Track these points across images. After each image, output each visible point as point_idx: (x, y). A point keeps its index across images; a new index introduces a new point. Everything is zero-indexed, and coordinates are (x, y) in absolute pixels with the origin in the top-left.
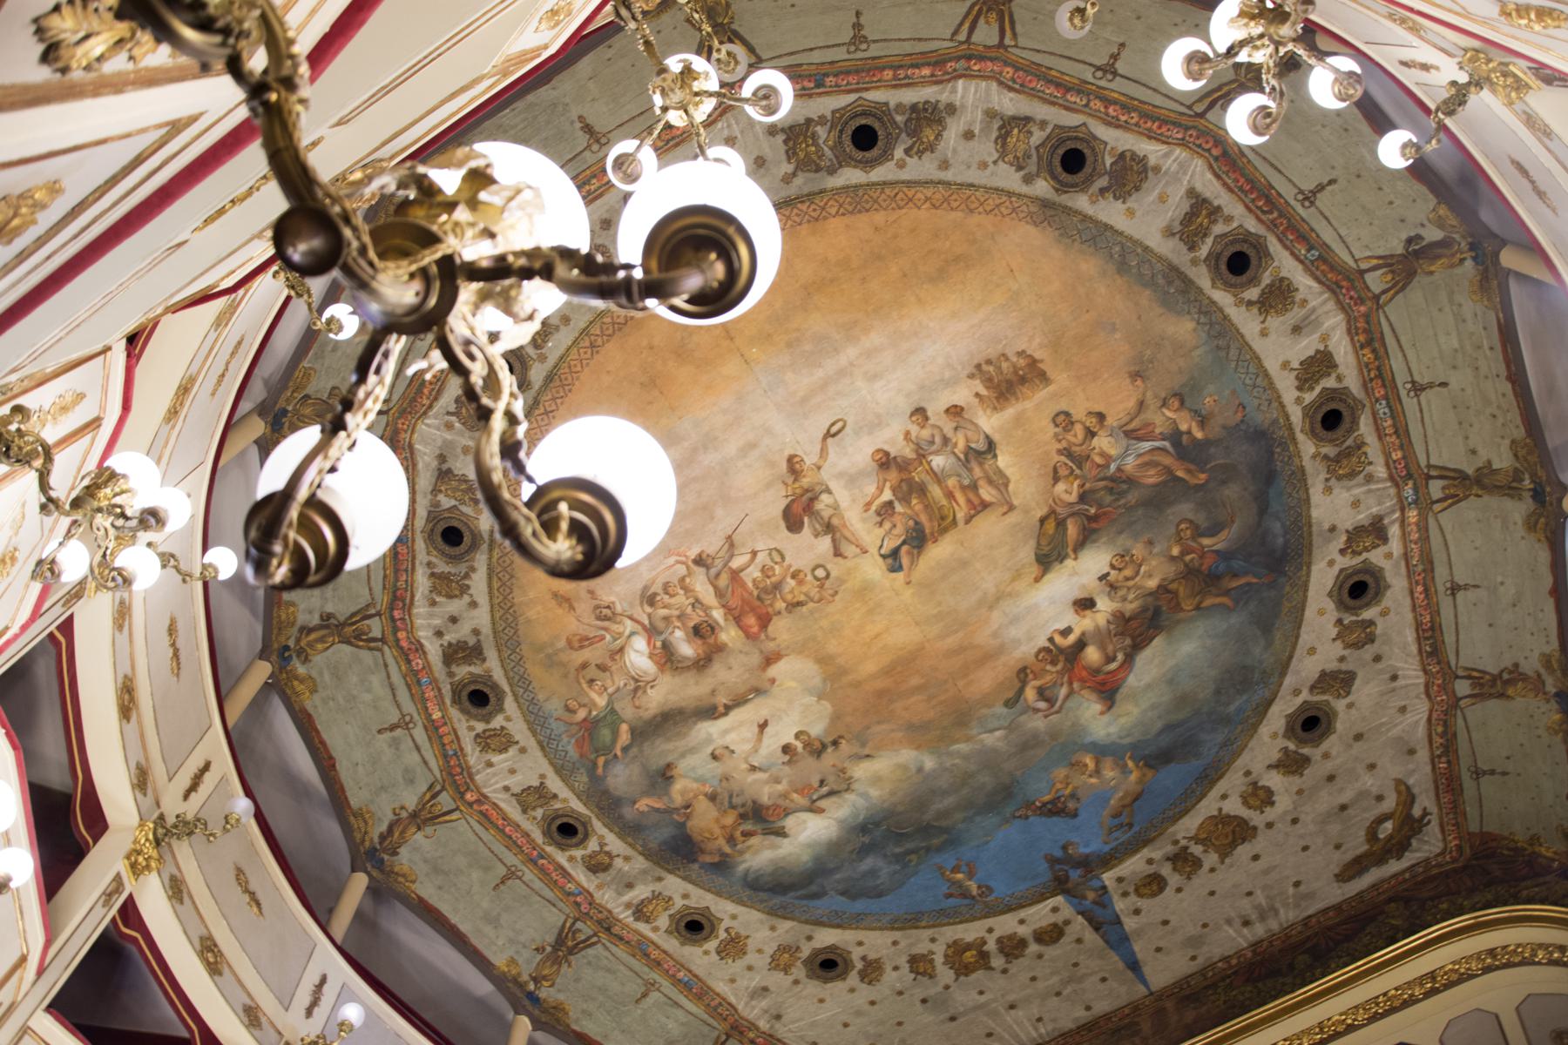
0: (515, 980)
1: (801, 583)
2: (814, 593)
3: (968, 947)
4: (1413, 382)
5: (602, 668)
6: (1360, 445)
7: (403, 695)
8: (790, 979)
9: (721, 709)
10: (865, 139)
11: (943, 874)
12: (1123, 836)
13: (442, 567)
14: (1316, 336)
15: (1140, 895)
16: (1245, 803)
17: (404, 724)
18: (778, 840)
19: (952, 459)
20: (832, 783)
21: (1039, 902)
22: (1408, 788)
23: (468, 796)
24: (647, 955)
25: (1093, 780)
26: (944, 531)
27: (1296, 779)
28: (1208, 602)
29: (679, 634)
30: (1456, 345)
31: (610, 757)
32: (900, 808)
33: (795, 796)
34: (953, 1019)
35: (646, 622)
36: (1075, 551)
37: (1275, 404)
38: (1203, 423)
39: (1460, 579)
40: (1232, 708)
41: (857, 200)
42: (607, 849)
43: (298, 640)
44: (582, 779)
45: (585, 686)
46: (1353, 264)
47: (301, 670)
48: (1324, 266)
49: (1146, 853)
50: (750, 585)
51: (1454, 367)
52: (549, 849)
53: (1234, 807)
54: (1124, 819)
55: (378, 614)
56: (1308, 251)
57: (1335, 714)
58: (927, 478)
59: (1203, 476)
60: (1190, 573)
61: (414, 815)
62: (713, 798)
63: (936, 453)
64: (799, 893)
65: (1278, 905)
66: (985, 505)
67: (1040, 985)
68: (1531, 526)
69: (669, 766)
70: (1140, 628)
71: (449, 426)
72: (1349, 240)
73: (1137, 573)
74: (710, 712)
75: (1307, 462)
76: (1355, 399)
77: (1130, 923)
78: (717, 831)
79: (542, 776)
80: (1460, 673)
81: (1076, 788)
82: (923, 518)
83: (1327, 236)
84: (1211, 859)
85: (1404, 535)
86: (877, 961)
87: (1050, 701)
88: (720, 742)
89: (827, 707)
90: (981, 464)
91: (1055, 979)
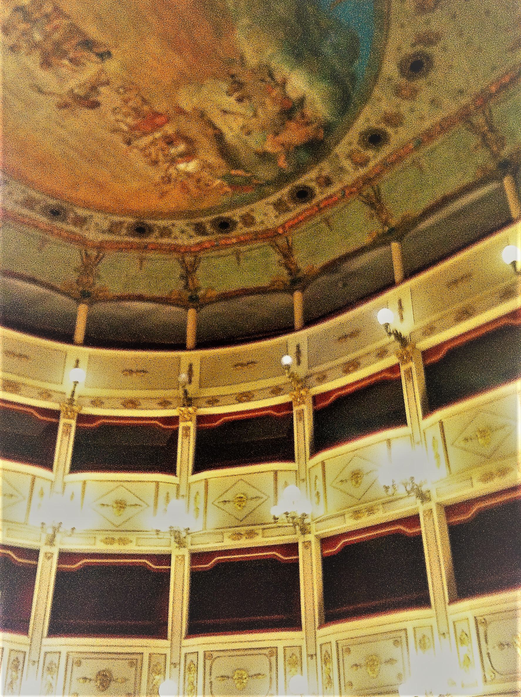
0: (379, 236)
7: (222, 252)
13: (157, 233)
17: (238, 254)
18: (307, 102)
23: (281, 231)
29: (173, 151)
32: (282, 35)
33: (274, 94)
43: (190, 290)
47: (202, 292)
52: (314, 202)
55: (183, 257)
61: (285, 256)
66: (56, 9)
69: (257, 153)
74: (219, 137)
82: (74, 42)
89: (209, 82)
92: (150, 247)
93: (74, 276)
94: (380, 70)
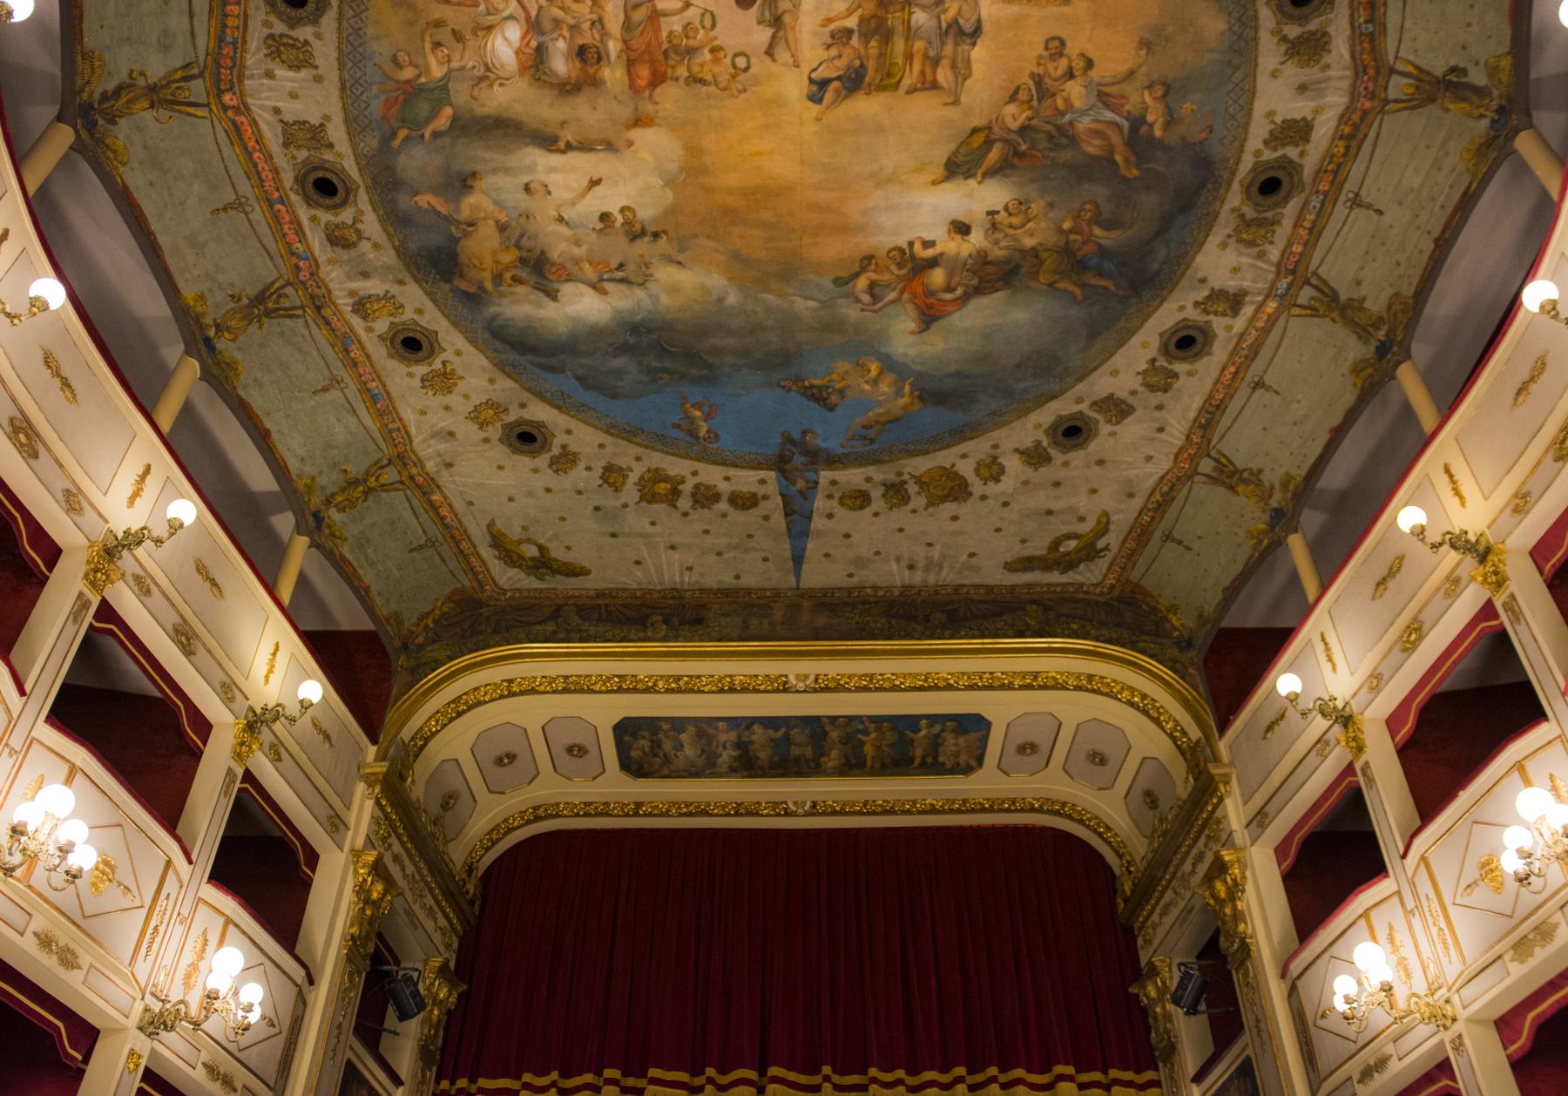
1: (716, 61)
3: (666, 479)
4: (1357, 195)
5: (458, 37)
6: (1275, 222)
8: (483, 435)
9: (562, 145)
11: (683, 405)
12: (860, 447)
14: (1313, 104)
15: (841, 503)
16: (977, 471)
19: (934, 23)
20: (630, 272)
21: (753, 468)
22: (1108, 522)
24: (347, 351)
25: (867, 387)
26: (882, 88)
27: (1029, 471)
28: (1061, 285)
29: (561, 44)
30: (1416, 186)
31: (415, 134)
34: (613, 535)
35: (533, 14)
36: (984, 175)
37: (1237, 144)
38: (1168, 124)
39: (1268, 380)
40: (1021, 385)
42: (359, 226)
44: (372, 142)
45: (428, 45)
46: (1391, 58)
49: (870, 471)
50: (664, 34)
51: (1400, 203)
53: (966, 469)
54: (871, 433)
56: (1366, 22)
57: (1097, 434)
58: (899, 28)
59: (1135, 172)
60: (1066, 251)
62: (502, 228)
63: (924, 8)
65: (945, 564)
66: (935, 86)
67: (709, 539)
68: (1356, 370)
69: (474, 174)
72: (1406, 35)
73: (1023, 226)
74: (548, 141)
75: (1225, 212)
76: (1301, 180)
77: (818, 522)
78: (489, 263)
79: (327, 118)
80: (1213, 454)
81: (847, 386)
82: (871, 66)
83: (1393, 18)
84: (919, 501)
86: (575, 454)
87: (875, 298)
88: (540, 176)
90: (956, 44)
91: (725, 541)
94: (551, 404)
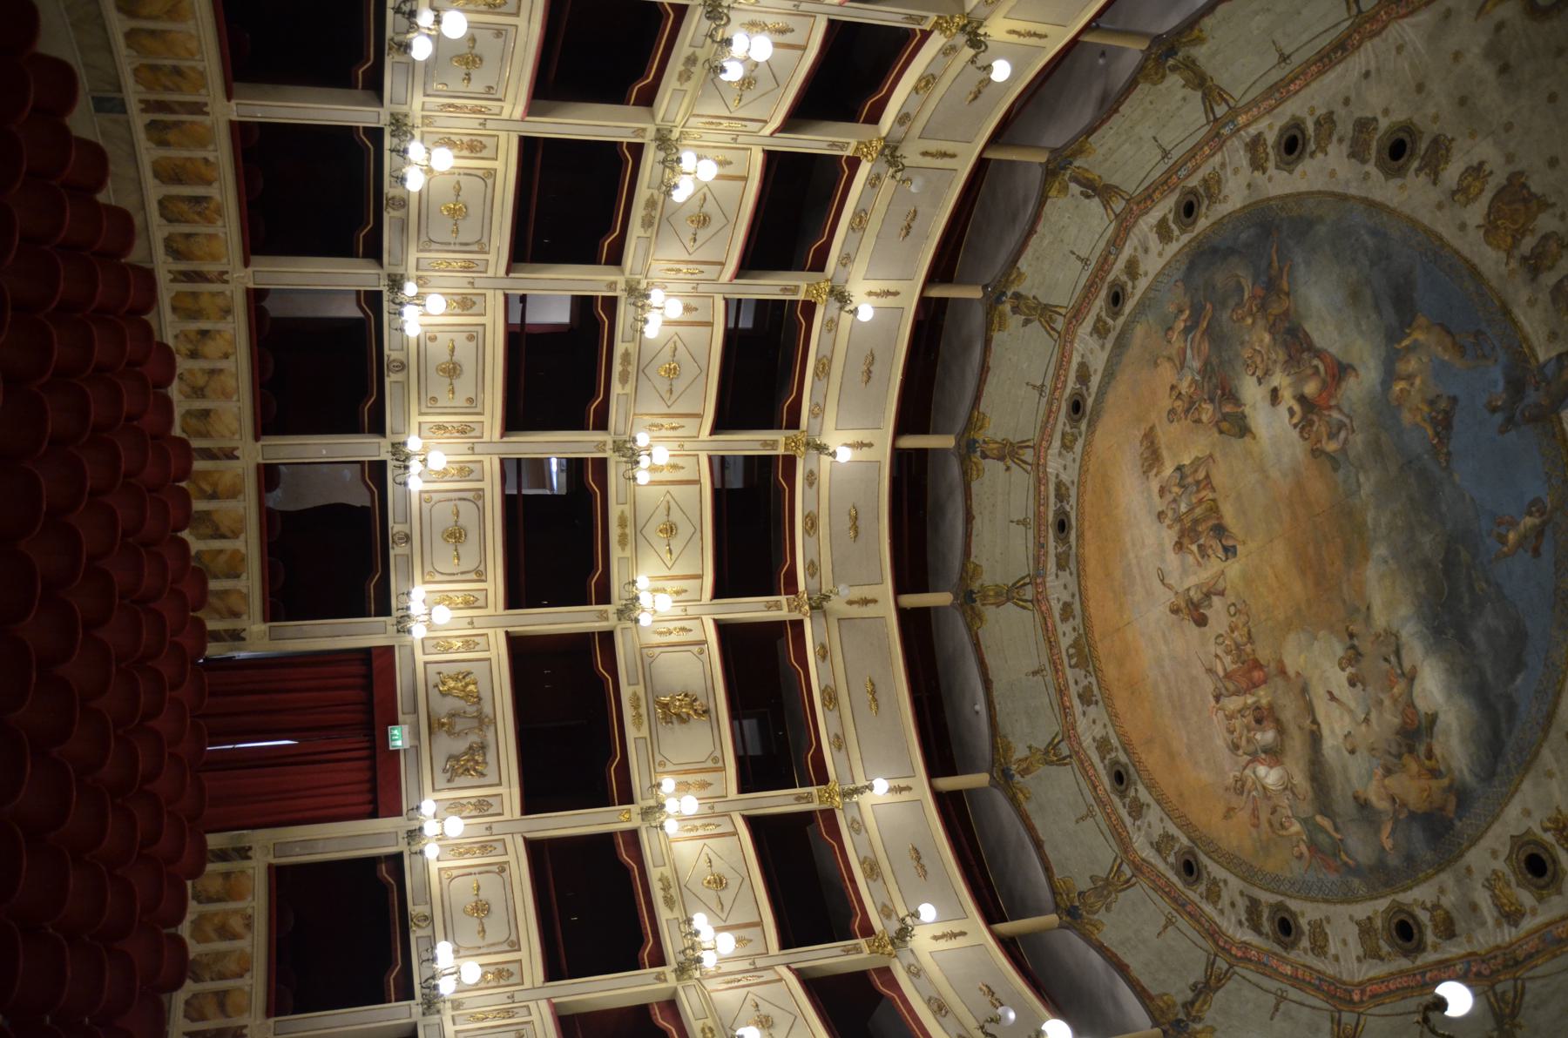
2: (1243, 618)
5: (1274, 811)
6: (1205, 181)
10: (1062, 526)
13: (1202, 888)
17: (1281, 998)
23: (1356, 998)
25: (1418, 382)
28: (1285, 286)
29: (1258, 736)
30: (1127, 146)
32: (1422, 589)
38: (1181, 311)
39: (1275, 58)
41: (1080, 536)
42: (1429, 905)
43: (1188, 1014)
48: (1116, 243)
52: (1419, 962)
53: (1476, 213)
59: (1209, 306)
62: (1388, 772)
64: (1504, 725)
66: (1207, 476)
68: (1200, 41)
69: (1356, 798)
70: (1295, 343)
71: (1139, 829)
72: (1100, 230)
74: (1315, 739)
78: (1424, 783)
80: (1354, 11)
83: (1102, 244)
84: (1546, 222)
85: (1256, 120)
92: (1189, 908)
93: (1084, 884)
94: (1556, 704)
